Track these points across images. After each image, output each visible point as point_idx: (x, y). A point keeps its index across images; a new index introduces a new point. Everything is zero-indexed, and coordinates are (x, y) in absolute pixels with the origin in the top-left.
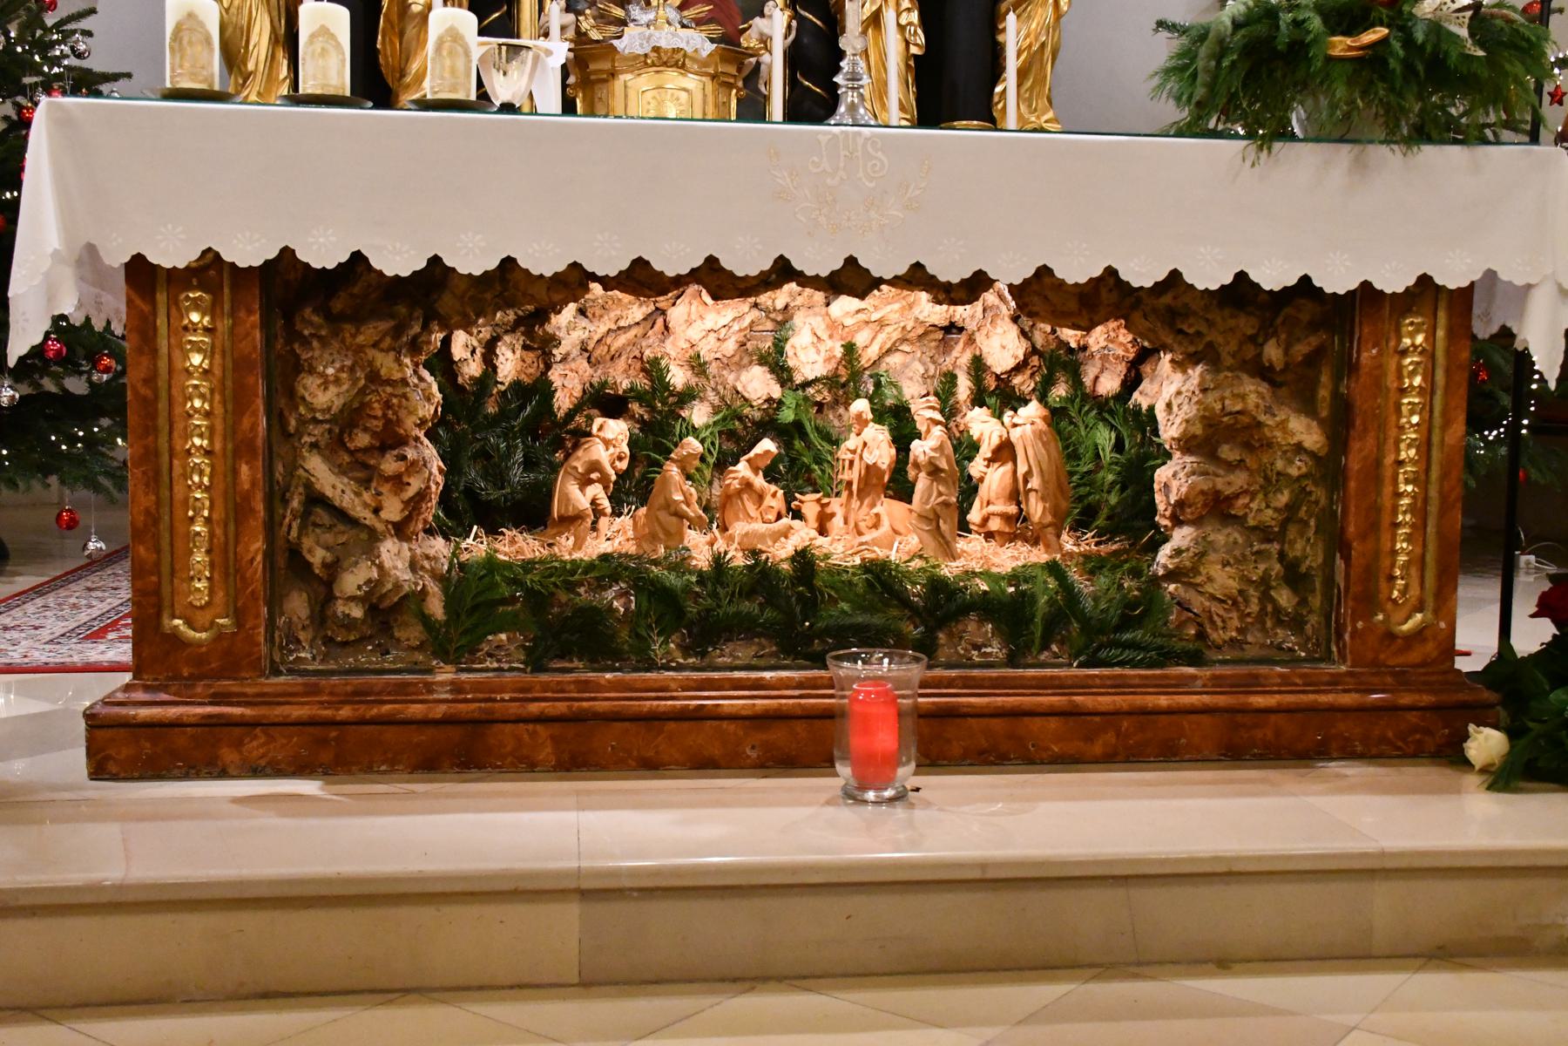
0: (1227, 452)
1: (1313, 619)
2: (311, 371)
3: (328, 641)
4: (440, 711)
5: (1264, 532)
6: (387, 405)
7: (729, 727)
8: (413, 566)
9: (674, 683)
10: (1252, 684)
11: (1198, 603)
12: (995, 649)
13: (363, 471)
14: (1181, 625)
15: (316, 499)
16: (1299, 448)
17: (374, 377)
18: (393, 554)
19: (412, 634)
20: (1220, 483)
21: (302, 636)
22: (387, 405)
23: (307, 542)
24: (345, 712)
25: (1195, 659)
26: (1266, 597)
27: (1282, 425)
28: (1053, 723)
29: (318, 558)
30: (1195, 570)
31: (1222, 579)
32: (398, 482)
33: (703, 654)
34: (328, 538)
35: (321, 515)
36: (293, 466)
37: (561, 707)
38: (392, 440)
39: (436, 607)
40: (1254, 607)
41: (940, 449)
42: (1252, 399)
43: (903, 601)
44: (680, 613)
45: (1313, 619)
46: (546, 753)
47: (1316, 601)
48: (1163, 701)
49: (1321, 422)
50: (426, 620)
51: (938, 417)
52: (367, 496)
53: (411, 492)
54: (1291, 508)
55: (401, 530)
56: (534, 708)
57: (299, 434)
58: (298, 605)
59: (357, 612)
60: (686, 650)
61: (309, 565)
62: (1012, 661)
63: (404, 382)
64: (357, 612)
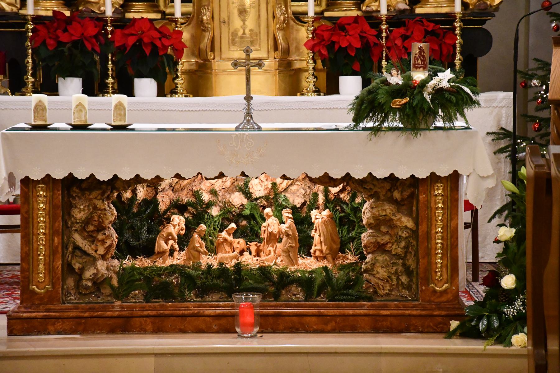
0: (383, 229)
1: (414, 286)
2: (76, 207)
3: (80, 293)
4: (116, 314)
5: (398, 256)
6: (99, 217)
7: (208, 319)
8: (108, 269)
9: (191, 304)
10: (385, 307)
11: (373, 280)
12: (301, 296)
13: (92, 239)
14: (368, 288)
15: (77, 248)
16: (406, 227)
17: (95, 208)
18: (101, 265)
19: (107, 291)
20: (379, 239)
21: (72, 292)
22: (99, 217)
23: (73, 262)
24: (87, 314)
25: (370, 299)
26: (398, 279)
27: (399, 219)
28: (314, 319)
29: (77, 266)
30: (372, 269)
31: (382, 272)
32: (103, 242)
33: (202, 297)
34: (80, 260)
35: (78, 253)
36: (69, 237)
37: (154, 313)
38: (101, 228)
39: (115, 282)
40: (395, 282)
41: (289, 227)
42: (388, 211)
43: (271, 280)
44: (195, 284)
45: (414, 286)
46: (149, 327)
47: (414, 280)
48: (351, 312)
49: (413, 219)
50: (112, 287)
51: (290, 216)
52: (93, 246)
53: (107, 245)
54: (406, 247)
55: (103, 257)
56: (146, 313)
57: (71, 227)
58: (70, 282)
59: (90, 284)
60: (197, 296)
61: (74, 269)
62: (306, 300)
63: (105, 209)
64: (90, 284)
